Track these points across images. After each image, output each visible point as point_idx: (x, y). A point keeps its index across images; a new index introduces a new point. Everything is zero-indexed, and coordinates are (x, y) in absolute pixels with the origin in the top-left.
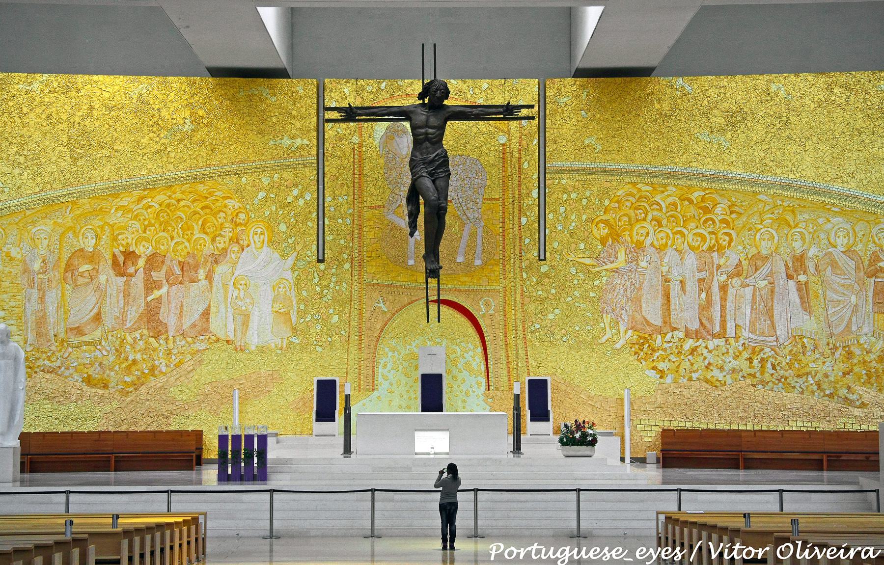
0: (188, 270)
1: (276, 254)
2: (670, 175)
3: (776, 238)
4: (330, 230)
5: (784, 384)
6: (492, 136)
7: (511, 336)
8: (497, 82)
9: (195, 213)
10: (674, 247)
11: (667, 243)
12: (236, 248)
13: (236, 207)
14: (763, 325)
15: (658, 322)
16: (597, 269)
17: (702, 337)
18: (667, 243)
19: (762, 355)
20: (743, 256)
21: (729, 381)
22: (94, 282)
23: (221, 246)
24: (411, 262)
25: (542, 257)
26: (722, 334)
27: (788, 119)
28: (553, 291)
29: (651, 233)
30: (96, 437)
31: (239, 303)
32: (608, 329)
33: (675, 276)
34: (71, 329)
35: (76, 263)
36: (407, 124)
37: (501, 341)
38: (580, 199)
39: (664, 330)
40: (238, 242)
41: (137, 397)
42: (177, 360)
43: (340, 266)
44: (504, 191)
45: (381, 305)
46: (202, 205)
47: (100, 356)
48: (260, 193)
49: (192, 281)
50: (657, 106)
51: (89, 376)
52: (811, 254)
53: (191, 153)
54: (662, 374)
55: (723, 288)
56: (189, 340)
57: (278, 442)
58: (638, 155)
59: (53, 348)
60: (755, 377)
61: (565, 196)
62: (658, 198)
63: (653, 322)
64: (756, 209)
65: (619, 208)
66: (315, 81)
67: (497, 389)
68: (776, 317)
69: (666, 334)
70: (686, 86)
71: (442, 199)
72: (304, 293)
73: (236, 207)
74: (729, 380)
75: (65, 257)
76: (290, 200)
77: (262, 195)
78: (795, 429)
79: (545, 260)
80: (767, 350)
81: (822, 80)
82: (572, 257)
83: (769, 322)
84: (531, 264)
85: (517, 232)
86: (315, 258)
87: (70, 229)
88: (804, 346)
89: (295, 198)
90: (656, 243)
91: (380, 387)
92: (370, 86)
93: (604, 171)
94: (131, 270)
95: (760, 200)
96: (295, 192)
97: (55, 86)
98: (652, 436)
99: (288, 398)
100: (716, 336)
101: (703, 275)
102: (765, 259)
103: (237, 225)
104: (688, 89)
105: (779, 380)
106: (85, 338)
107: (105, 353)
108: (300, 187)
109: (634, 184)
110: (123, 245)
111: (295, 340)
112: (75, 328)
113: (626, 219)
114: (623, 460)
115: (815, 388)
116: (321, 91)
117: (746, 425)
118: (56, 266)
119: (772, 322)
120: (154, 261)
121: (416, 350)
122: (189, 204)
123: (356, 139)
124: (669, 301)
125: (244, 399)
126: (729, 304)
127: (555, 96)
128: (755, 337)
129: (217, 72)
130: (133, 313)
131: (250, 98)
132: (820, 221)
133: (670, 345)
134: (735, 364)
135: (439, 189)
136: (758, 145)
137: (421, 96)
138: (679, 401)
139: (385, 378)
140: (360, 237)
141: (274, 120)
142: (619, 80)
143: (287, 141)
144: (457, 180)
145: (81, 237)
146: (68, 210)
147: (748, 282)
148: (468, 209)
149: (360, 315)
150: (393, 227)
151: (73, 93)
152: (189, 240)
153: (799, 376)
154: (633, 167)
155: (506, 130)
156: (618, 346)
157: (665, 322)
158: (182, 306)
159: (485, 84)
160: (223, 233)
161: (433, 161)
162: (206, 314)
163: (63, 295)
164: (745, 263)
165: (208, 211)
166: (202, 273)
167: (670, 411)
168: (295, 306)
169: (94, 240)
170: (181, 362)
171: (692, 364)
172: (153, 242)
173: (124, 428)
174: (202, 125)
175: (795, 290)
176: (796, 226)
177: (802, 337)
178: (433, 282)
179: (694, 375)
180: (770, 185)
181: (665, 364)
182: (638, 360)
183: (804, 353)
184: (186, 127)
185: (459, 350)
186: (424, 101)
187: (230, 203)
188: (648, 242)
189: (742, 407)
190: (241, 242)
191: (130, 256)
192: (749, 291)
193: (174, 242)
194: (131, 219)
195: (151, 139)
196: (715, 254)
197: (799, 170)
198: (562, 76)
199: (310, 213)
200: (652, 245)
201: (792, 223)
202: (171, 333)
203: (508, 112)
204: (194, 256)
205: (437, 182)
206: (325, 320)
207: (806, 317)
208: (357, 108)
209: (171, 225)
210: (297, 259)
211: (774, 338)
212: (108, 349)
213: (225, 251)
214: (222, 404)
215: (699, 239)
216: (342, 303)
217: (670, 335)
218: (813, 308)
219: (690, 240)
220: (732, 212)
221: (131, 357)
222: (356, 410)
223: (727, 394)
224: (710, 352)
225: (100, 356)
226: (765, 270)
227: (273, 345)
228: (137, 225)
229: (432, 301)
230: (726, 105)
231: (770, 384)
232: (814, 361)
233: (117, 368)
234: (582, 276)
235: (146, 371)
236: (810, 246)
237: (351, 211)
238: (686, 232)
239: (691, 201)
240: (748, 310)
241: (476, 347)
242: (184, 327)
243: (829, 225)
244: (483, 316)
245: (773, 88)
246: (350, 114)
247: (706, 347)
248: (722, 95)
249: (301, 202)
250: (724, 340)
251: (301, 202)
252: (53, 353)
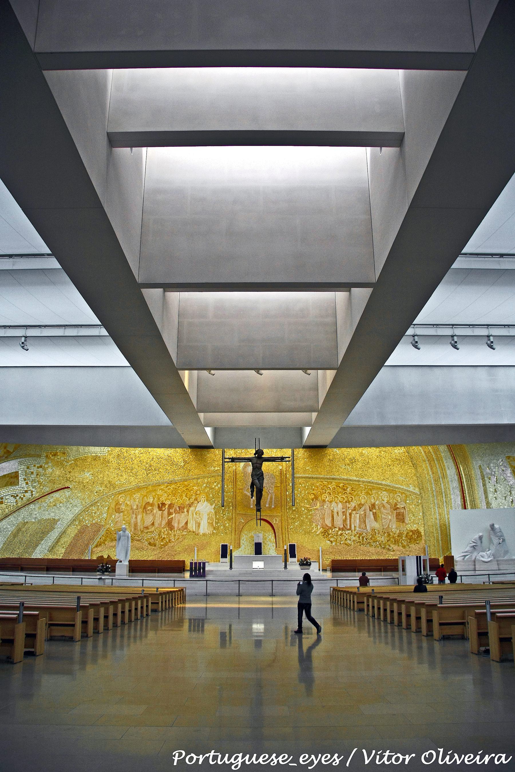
0: (181, 509)
1: (209, 504)
2: (333, 479)
3: (366, 498)
4: (226, 496)
5: (369, 545)
6: (277, 467)
7: (284, 530)
8: (278, 450)
9: (184, 491)
10: (335, 501)
11: (332, 500)
12: (196, 502)
13: (197, 489)
14: (363, 526)
15: (330, 525)
16: (311, 509)
17: (344, 530)
18: (332, 500)
19: (363, 535)
20: (356, 504)
21: (352, 544)
22: (152, 512)
23: (192, 501)
24: (252, 507)
25: (293, 505)
26: (350, 529)
27: (368, 461)
28: (297, 516)
29: (328, 497)
30: (152, 562)
31: (197, 519)
32: (314, 528)
33: (335, 511)
34: (145, 527)
35: (147, 506)
36: (250, 463)
37: (280, 531)
38: (305, 486)
39: (332, 528)
40: (197, 500)
41: (165, 549)
42: (177, 538)
43: (229, 508)
44: (281, 484)
45: (242, 520)
46: (186, 488)
47: (154, 536)
48: (204, 485)
49: (183, 512)
50: (329, 457)
51: (150, 542)
52: (377, 503)
53: (183, 472)
54: (331, 542)
57: (209, 564)
58: (323, 472)
59: (139, 533)
60: (360, 542)
61: (300, 485)
62: (329, 486)
63: (328, 525)
64: (360, 489)
65: (318, 489)
66: (222, 450)
67: (279, 547)
68: (367, 523)
69: (333, 529)
70: (337, 451)
71: (261, 486)
72: (218, 517)
73: (197, 489)
74: (352, 544)
75: (144, 505)
76: (213, 487)
77: (205, 485)
78: (373, 559)
79: (294, 506)
80: (364, 534)
81: (378, 449)
82: (303, 505)
83: (364, 525)
84: (290, 507)
85: (285, 497)
86: (221, 505)
87: (145, 496)
88: (375, 532)
89: (215, 486)
90: (329, 500)
91: (241, 547)
92: (239, 451)
93: (313, 477)
94: (164, 509)
95: (361, 487)
96: (215, 484)
97: (143, 452)
98: (328, 562)
99: (212, 550)
100: (348, 530)
101: (344, 510)
102: (363, 505)
103: (197, 495)
104: (338, 452)
105: (368, 543)
106: (149, 530)
107: (155, 535)
108: (217, 483)
109: (322, 482)
110: (161, 501)
111: (215, 532)
112: (146, 527)
113: (319, 492)
114: (319, 570)
115: (379, 546)
116: (223, 453)
117: (358, 558)
118: (141, 507)
119: (366, 525)
120: (171, 506)
121: (253, 535)
122: (182, 488)
123: (234, 468)
124: (333, 519)
125: (198, 551)
126: (352, 519)
127: (297, 454)
128: (360, 530)
129: (192, 447)
130: (164, 523)
131: (202, 455)
132: (379, 493)
133: (334, 532)
134: (354, 538)
135: (261, 484)
136: (360, 469)
137: (255, 454)
138: (337, 551)
139: (243, 544)
140: (235, 499)
141: (209, 462)
142: (316, 449)
143: (213, 468)
144: (266, 481)
145: (148, 499)
146: (145, 490)
147: (358, 512)
148: (270, 489)
149: (235, 525)
150: (246, 495)
151: (148, 454)
152: (182, 500)
153: (374, 542)
154: (322, 476)
155: (282, 465)
156: (318, 533)
157: (332, 525)
158: (179, 521)
159: (275, 450)
160: (192, 497)
161: (259, 474)
162: (186, 523)
163: (143, 517)
165: (188, 490)
166: (185, 510)
167: (334, 554)
168: (215, 521)
169: (152, 500)
170: (179, 538)
171: (341, 539)
172: (171, 500)
173: (160, 559)
174: (186, 463)
175: (372, 515)
176: (372, 494)
177: (375, 530)
178: (258, 513)
179: (342, 542)
180: (363, 482)
181: (333, 539)
182: (324, 538)
183: (375, 535)
184: (182, 464)
185: (267, 535)
186: (256, 456)
187: (195, 488)
188: (327, 500)
189: (357, 552)
190: (198, 500)
191: (163, 504)
192: (358, 515)
193: (177, 500)
194: (164, 493)
195: (171, 468)
196: (347, 504)
197: (372, 477)
198: (299, 448)
199: (220, 491)
200: (328, 501)
201: (371, 494)
202: (176, 529)
203: (282, 459)
204: (183, 504)
205: (260, 481)
206: (224, 526)
207: (376, 523)
208: (235, 458)
209: (176, 495)
210: (215, 505)
211: (366, 530)
212: (156, 534)
213: (193, 503)
214: (191, 552)
215: (343, 499)
216: (230, 519)
217: (334, 530)
218: (378, 520)
219: (340, 499)
220: (352, 490)
221: (163, 537)
222: (234, 554)
223: (352, 548)
224: (346, 535)
225: (154, 536)
226: (363, 508)
227: (208, 533)
228: (166, 495)
229: (258, 519)
230: (349, 457)
231: (365, 545)
232: (379, 537)
233: (159, 540)
234: (306, 511)
235: (168, 541)
236: (376, 501)
237: (232, 490)
238: (338, 497)
239: (339, 487)
240: (358, 521)
241: (272, 534)
243: (382, 494)
244: (275, 524)
245: (364, 452)
246: (233, 460)
247: (345, 533)
248: (348, 454)
249: (217, 488)
250: (351, 531)
251: (217, 488)
252: (139, 535)
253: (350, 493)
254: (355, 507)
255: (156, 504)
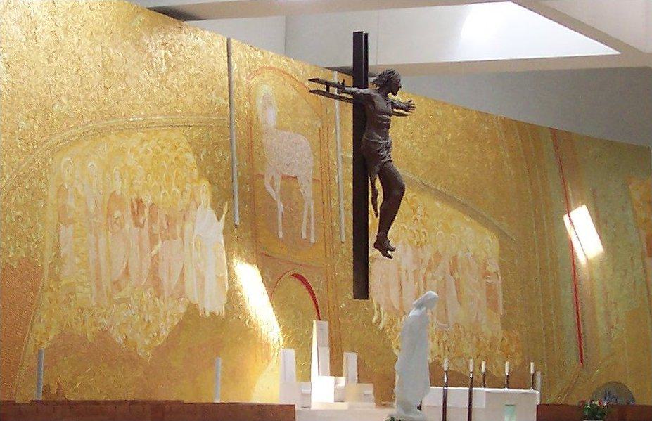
33: (403, 267)
55: (424, 279)
56: (176, 302)
101: (415, 267)
156: (381, 326)
157: (400, 307)
162: (182, 275)
164: (433, 259)
211: (446, 325)
213: (188, 207)
226: (441, 265)
242: (173, 288)
253: (422, 222)
254: (430, 260)
255: (129, 203)
